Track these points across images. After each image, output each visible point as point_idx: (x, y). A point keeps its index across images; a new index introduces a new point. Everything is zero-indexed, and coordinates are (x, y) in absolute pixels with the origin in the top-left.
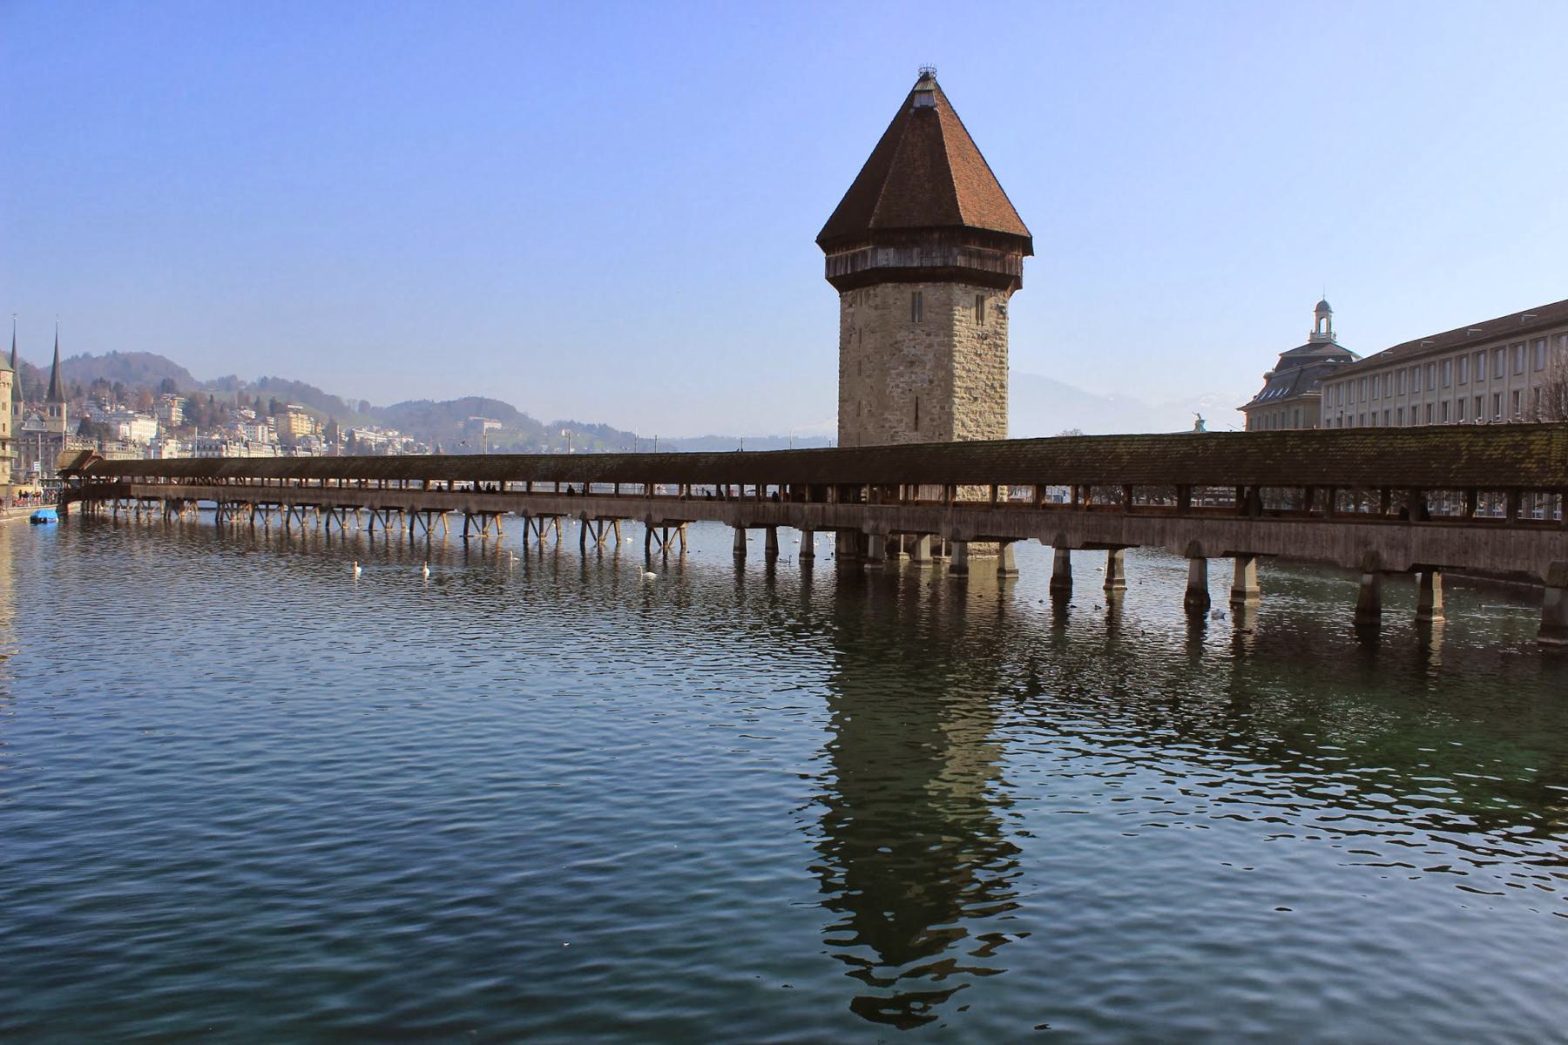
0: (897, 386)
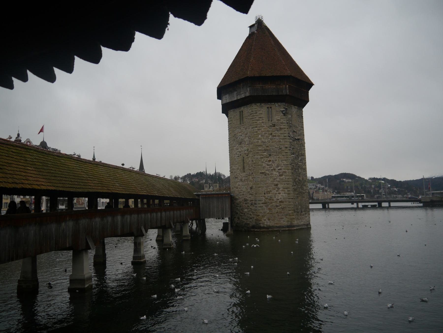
0: (236, 154)
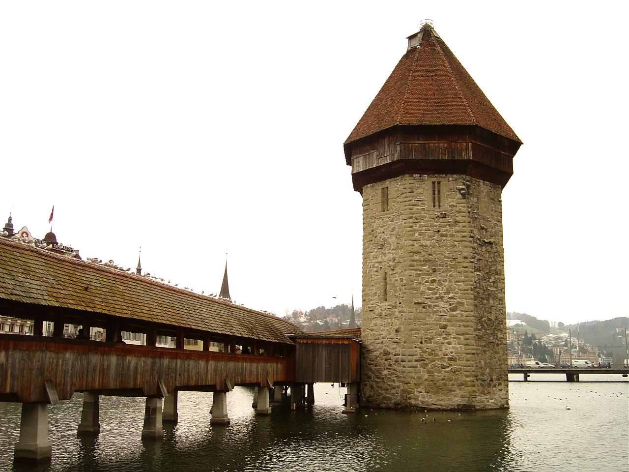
0: (374, 267)
